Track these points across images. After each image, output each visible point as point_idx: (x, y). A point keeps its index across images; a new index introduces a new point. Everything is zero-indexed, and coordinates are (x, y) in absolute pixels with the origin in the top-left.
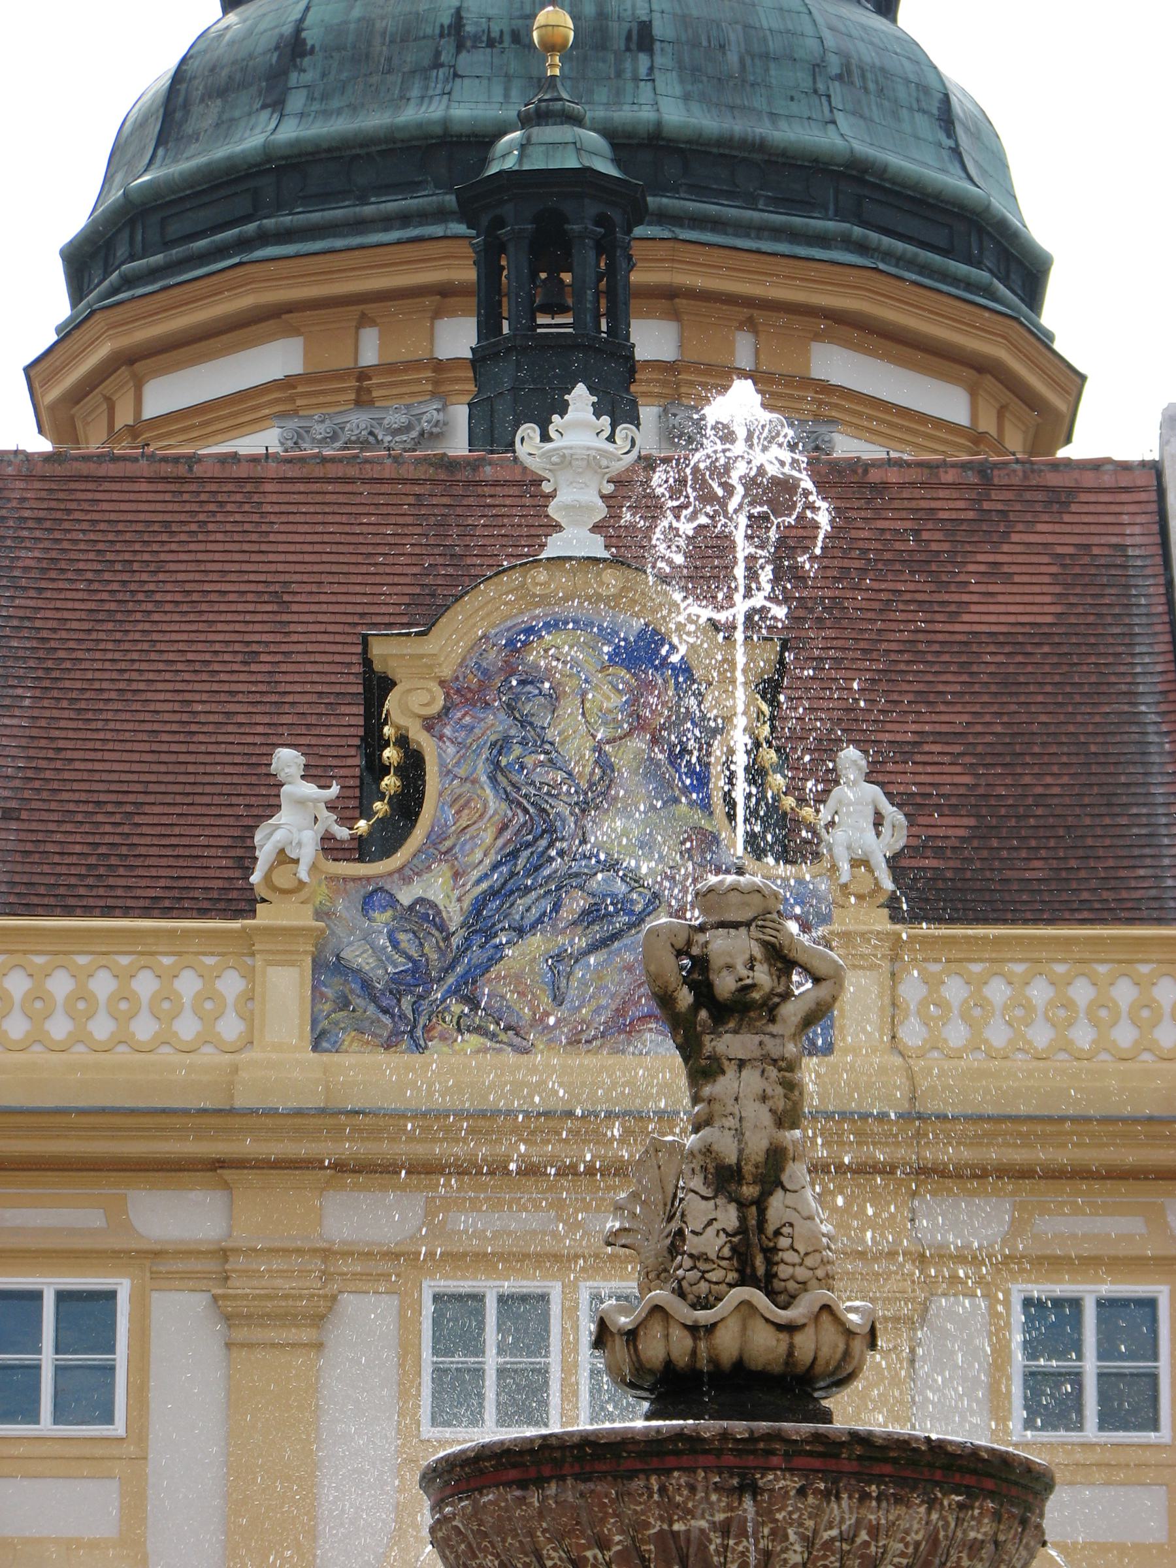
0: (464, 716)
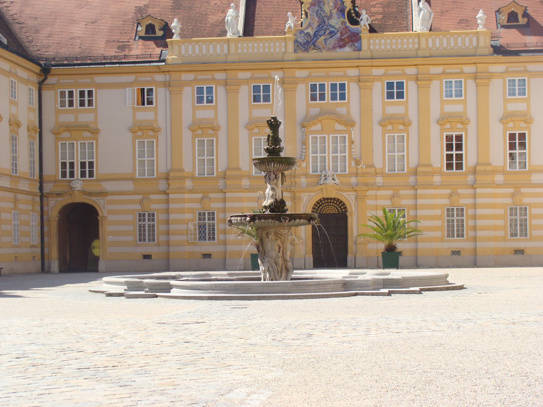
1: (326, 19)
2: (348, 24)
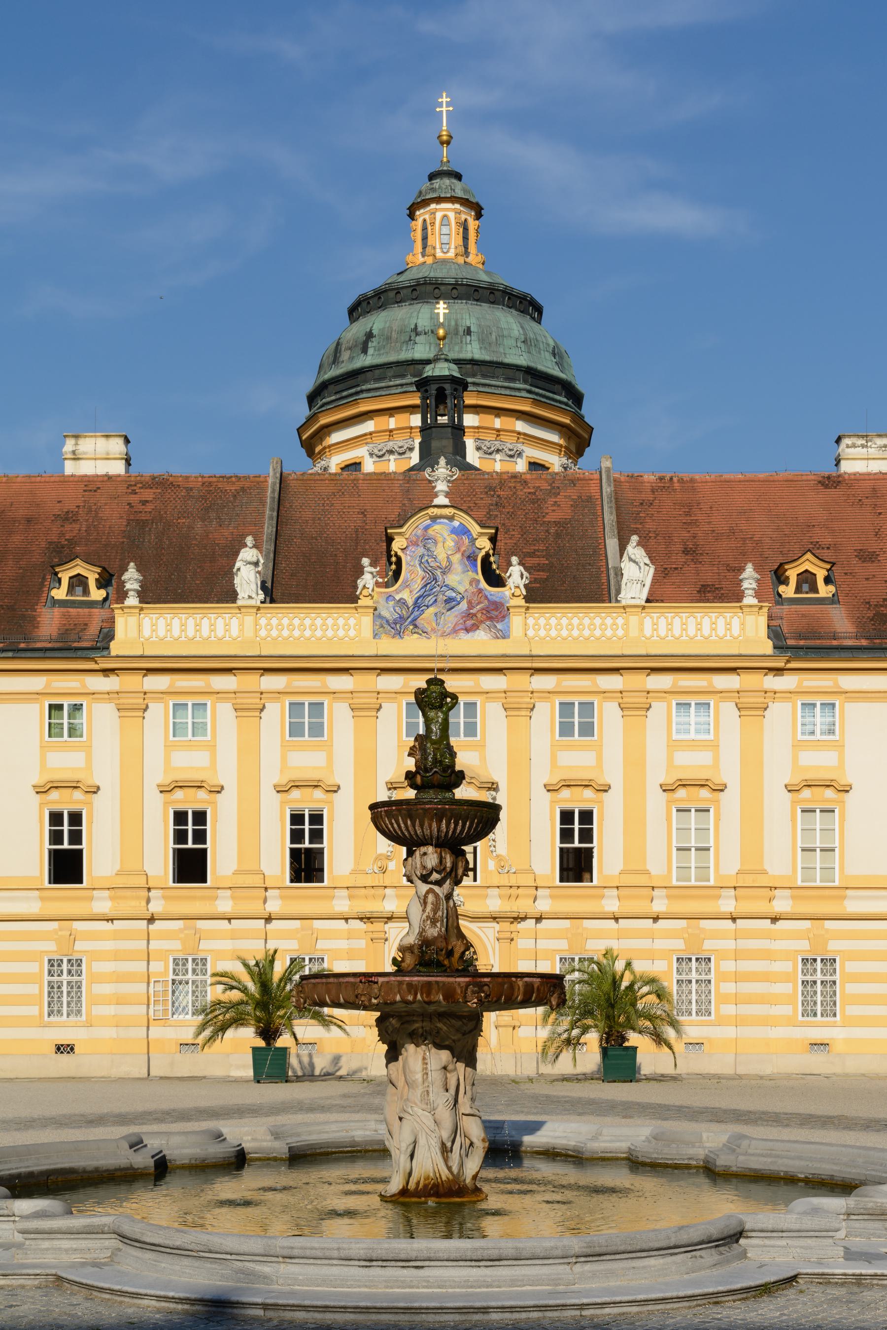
1: (438, 573)
2: (483, 584)
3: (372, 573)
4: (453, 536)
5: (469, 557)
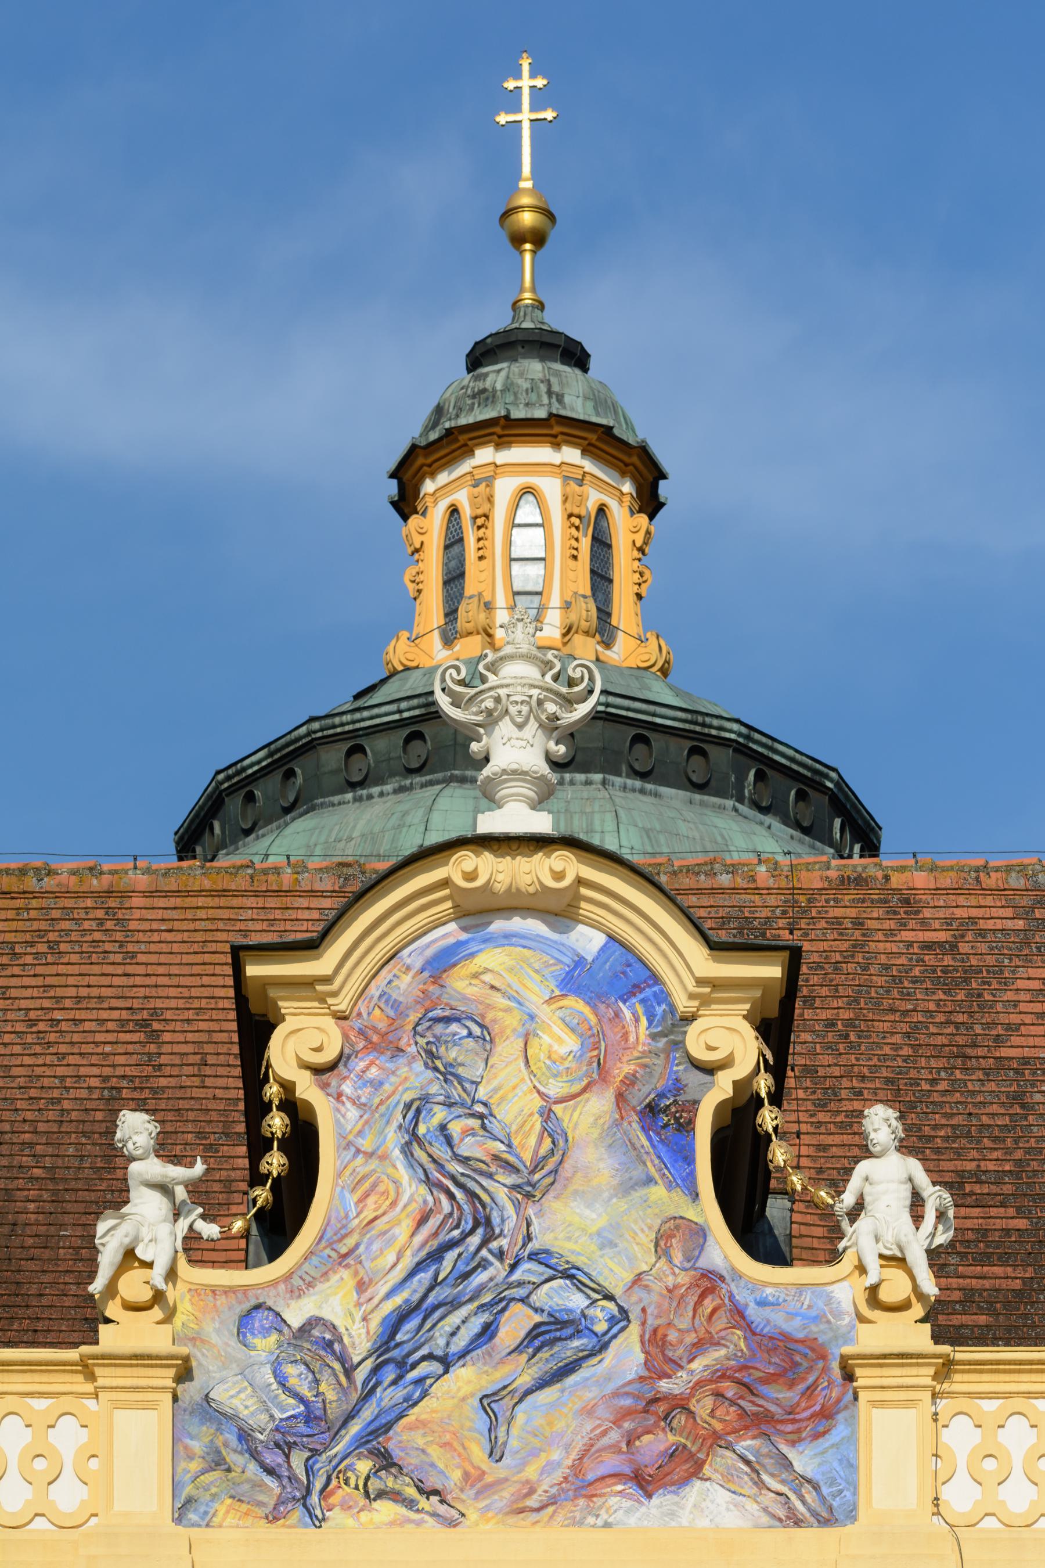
0: (368, 1068)
3: (164, 1189)
4: (576, 1004)
5: (651, 1110)
